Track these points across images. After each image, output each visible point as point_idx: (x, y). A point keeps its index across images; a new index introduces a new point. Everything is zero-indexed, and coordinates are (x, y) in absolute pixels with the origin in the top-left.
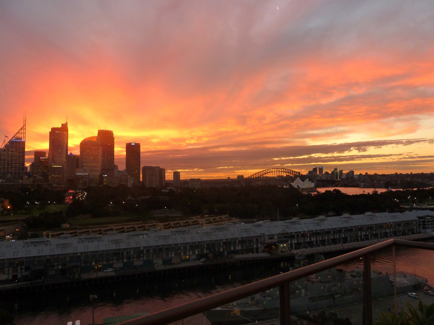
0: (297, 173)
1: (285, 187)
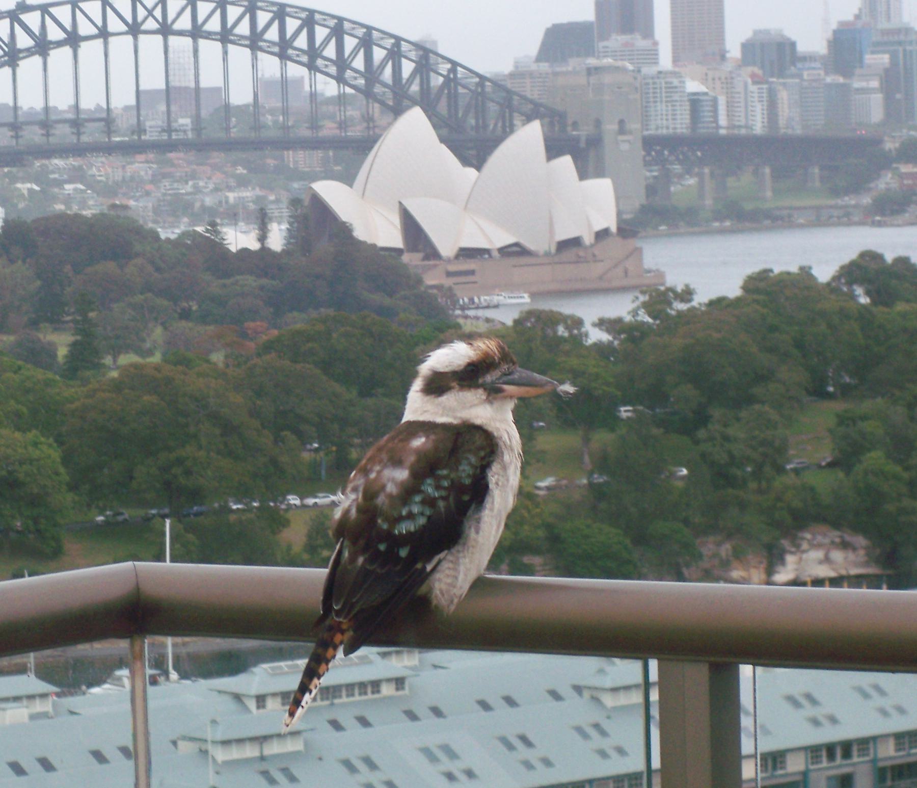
0: (395, 54)
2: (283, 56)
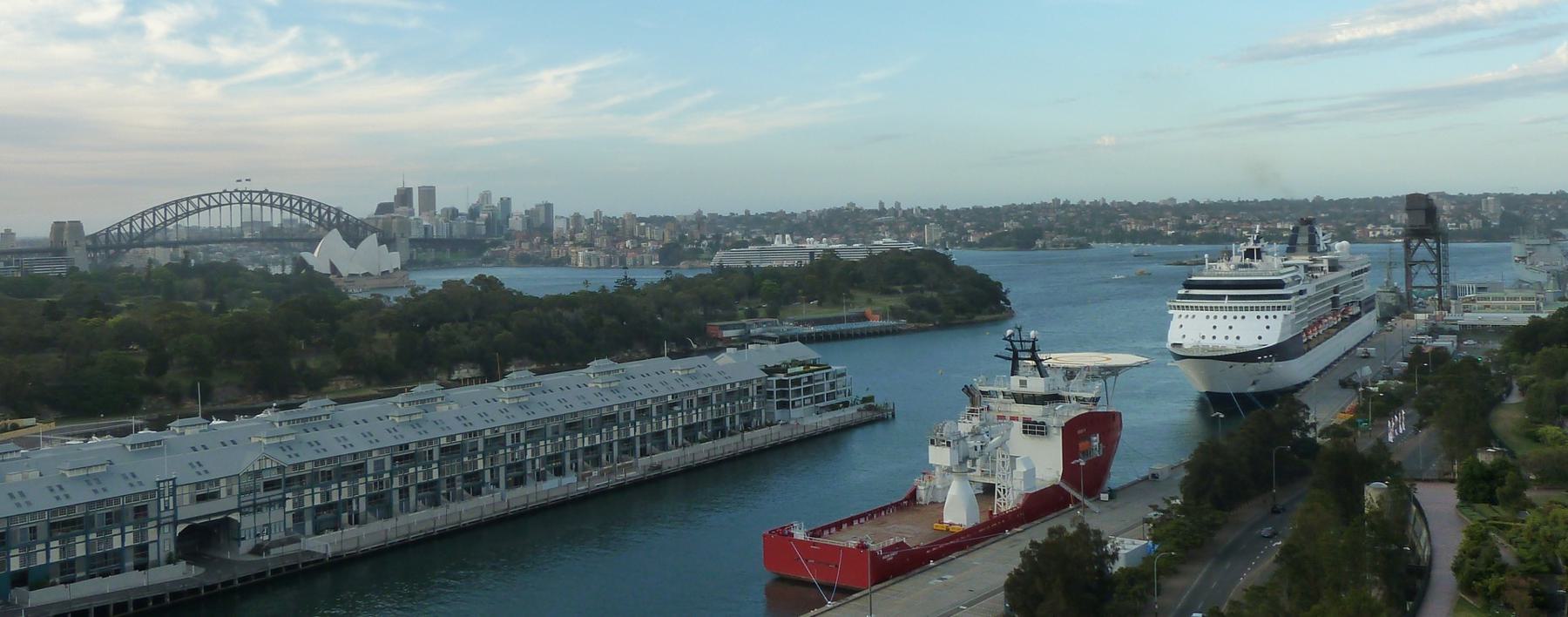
1: (275, 270)
2: (291, 212)
